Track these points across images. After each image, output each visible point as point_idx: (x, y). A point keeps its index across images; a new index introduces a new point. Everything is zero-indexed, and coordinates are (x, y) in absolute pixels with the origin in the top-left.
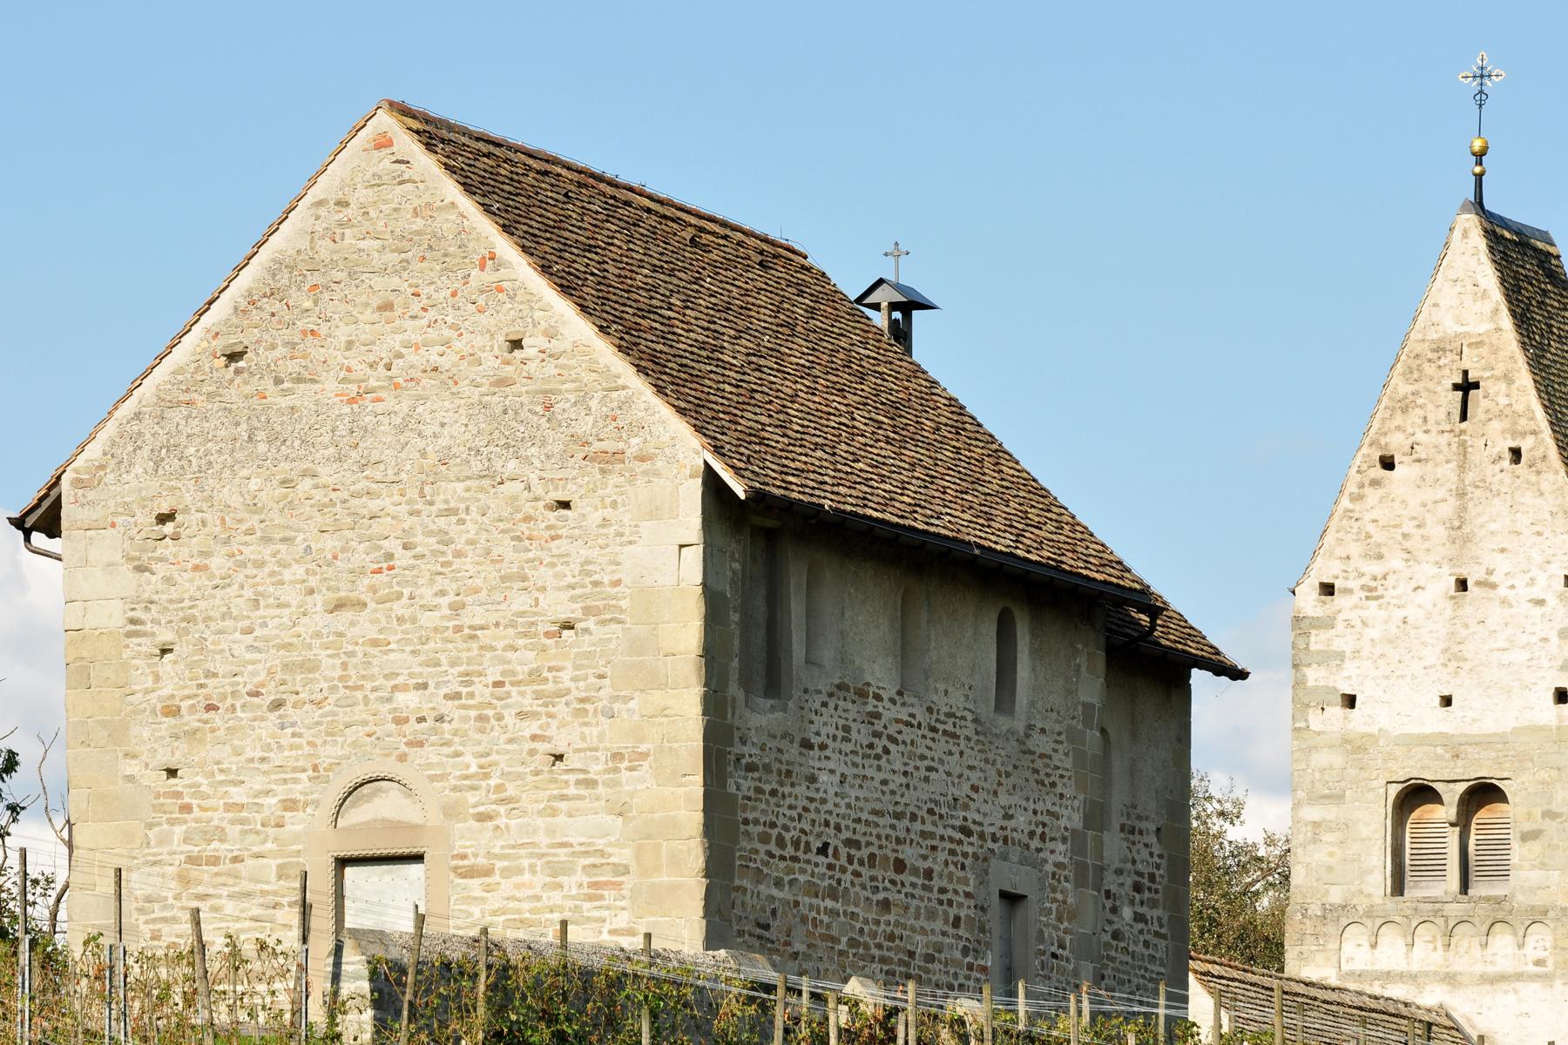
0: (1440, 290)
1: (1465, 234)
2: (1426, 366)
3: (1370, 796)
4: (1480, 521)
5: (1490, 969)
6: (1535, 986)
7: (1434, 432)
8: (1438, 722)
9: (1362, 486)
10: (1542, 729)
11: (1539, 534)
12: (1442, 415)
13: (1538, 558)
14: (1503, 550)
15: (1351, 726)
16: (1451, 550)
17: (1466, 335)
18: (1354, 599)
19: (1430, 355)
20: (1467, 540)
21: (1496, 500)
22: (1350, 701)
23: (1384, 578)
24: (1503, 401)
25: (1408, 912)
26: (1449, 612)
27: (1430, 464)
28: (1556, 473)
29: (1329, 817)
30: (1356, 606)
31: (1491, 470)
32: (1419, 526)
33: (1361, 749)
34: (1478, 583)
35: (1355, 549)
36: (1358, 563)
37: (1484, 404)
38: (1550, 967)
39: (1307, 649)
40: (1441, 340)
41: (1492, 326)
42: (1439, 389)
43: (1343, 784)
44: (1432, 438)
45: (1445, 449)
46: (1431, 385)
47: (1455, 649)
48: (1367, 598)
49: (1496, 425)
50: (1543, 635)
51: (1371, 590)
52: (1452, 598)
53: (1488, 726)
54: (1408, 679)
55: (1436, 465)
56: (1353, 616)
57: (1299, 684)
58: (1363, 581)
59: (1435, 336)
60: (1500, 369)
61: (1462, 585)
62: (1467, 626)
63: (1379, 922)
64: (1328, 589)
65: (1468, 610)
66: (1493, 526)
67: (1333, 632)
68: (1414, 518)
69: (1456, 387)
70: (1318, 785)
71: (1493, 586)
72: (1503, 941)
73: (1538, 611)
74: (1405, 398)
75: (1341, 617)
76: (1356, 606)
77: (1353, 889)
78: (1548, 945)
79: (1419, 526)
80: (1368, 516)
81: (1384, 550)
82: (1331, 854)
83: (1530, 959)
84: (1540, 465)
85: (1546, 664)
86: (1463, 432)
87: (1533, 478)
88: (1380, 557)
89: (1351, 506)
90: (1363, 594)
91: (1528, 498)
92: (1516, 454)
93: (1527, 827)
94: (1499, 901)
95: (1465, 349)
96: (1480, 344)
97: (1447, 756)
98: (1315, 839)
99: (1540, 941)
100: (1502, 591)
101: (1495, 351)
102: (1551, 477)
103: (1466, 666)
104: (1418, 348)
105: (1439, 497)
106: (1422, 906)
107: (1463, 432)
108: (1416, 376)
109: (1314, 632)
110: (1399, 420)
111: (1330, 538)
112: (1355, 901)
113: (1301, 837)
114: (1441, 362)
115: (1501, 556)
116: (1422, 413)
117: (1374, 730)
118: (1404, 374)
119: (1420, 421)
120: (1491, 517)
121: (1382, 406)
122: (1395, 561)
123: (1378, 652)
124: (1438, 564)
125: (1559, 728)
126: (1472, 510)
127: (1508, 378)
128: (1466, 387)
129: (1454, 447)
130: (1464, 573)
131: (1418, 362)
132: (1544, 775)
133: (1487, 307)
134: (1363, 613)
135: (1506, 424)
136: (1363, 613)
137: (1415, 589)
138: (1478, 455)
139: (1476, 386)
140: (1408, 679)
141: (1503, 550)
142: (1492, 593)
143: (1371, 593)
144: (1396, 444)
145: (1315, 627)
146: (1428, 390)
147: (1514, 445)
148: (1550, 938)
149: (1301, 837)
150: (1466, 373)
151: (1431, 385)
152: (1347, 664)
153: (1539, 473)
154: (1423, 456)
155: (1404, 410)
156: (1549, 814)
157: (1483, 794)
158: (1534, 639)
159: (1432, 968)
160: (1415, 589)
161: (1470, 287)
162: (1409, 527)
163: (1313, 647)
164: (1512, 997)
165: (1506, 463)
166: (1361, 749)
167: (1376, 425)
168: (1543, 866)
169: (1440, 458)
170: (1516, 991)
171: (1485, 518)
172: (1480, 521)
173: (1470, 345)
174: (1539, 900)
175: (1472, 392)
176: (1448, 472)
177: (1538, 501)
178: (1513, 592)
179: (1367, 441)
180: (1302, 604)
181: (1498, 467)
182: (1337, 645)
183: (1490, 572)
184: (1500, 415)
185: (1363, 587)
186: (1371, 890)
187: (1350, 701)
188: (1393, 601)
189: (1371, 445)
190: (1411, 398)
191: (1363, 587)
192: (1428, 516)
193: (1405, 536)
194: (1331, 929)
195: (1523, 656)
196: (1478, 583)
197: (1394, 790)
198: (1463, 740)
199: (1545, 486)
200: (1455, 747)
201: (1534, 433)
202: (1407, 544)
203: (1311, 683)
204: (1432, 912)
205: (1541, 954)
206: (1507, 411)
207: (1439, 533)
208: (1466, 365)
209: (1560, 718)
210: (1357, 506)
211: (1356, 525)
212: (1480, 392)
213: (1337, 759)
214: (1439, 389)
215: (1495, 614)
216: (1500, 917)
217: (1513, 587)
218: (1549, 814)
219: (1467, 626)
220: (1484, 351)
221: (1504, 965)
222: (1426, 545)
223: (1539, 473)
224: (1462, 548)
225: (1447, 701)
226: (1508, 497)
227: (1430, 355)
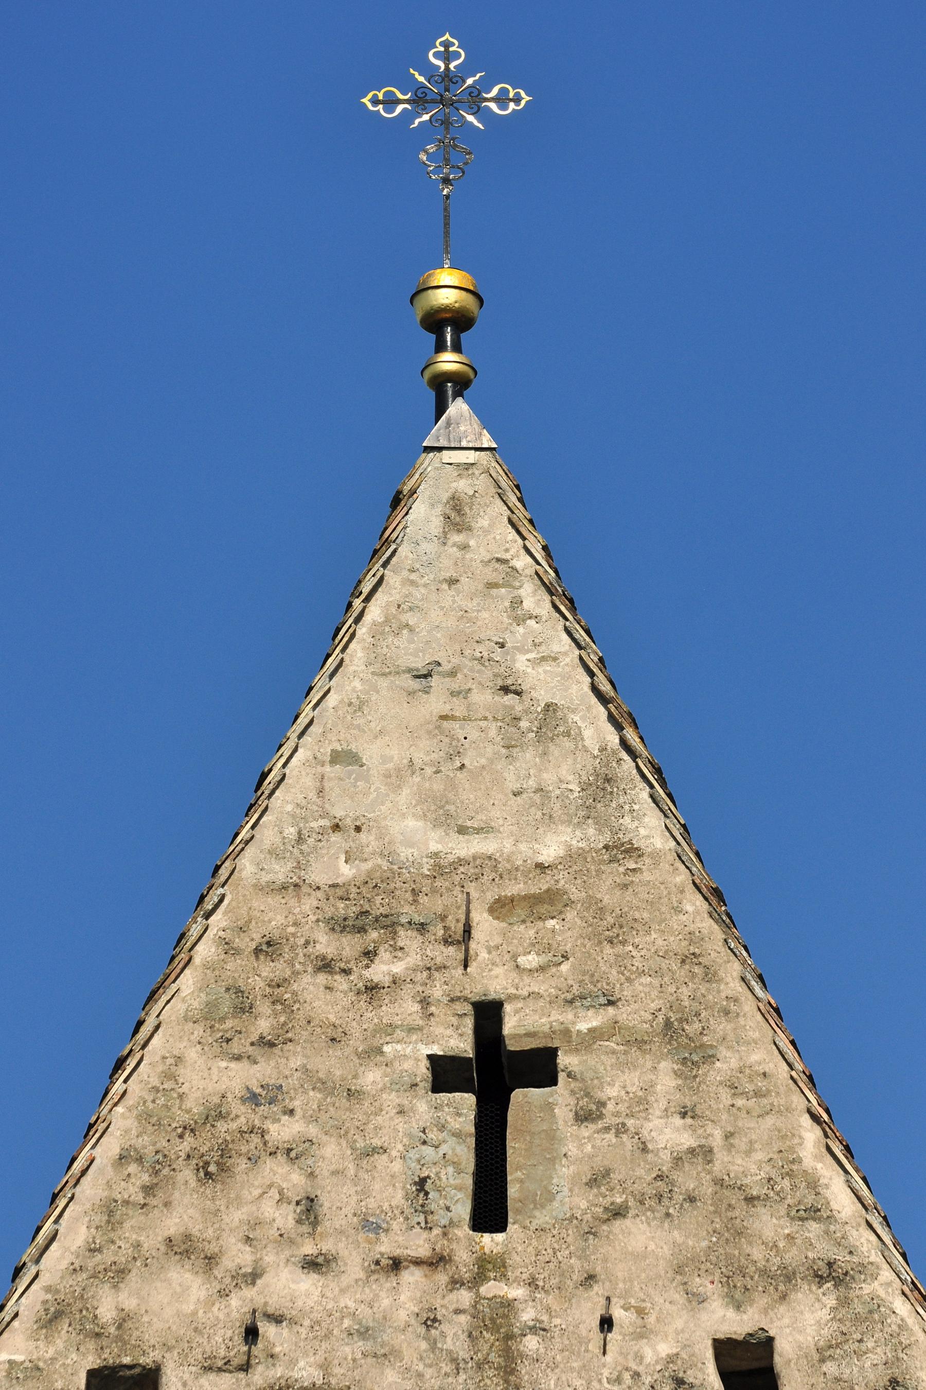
1: (457, 516)
2: (310, 986)
7: (353, 1265)
12: (388, 1192)
17: (484, 865)
19: (326, 944)
24: (669, 1135)
37: (581, 1146)
40: (374, 883)
41: (593, 837)
42: (371, 1078)
44: (345, 1294)
45: (412, 1346)
46: (331, 1064)
49: (640, 1235)
59: (346, 871)
60: (641, 1007)
69: (445, 1074)
74: (216, 1114)
86: (488, 1267)
96: (544, 904)
101: (614, 931)
104: (274, 917)
108: (264, 1026)
110: (184, 1212)
114: (382, 969)
116: (294, 1180)
118: (208, 1015)
119: (285, 1218)
127: (682, 1041)
128: (495, 1071)
129: (454, 1335)
131: (269, 969)
133: (564, 772)
135: (692, 1235)
139: (540, 1067)
146: (324, 1085)
147: (737, 1324)
150: (488, 1015)
151: (331, 1064)
155: (213, 1170)
161: (484, 698)
173: (501, 907)
175: (524, 1100)
184: (662, 1196)
189: (50, 1319)
190: (243, 1116)
201: (829, 1274)
206: (689, 1179)
208: (493, 981)
212: (560, 1097)
214: (371, 1078)
220: (563, 929)
227: (326, 944)
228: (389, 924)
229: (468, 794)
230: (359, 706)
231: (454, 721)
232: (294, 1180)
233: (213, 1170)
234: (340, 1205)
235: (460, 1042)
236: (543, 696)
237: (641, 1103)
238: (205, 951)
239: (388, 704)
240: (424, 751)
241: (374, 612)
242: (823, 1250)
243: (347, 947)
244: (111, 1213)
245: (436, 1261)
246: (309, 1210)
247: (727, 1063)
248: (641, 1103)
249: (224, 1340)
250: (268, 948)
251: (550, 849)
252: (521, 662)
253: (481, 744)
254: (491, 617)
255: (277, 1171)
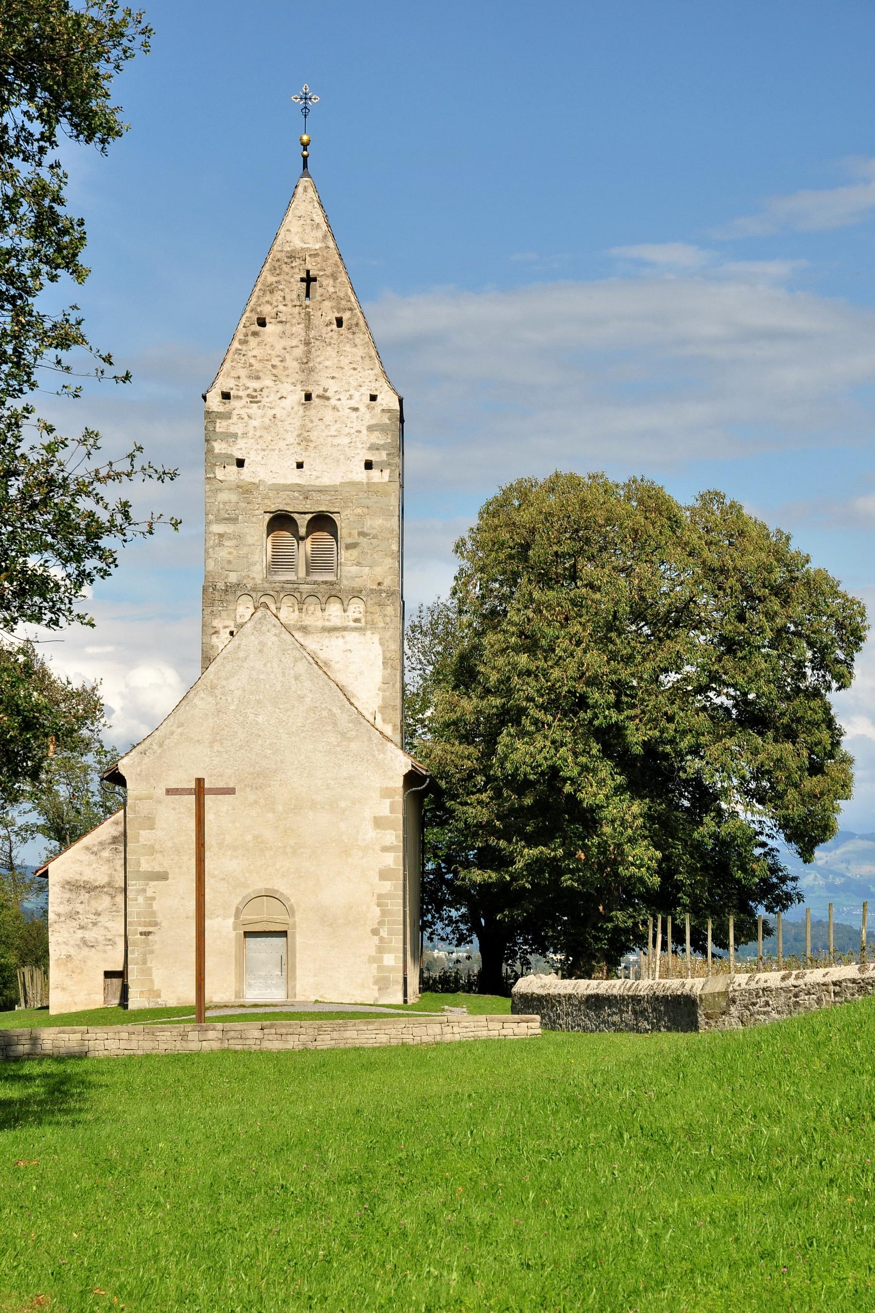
0: (291, 222)
1: (305, 190)
2: (284, 266)
3: (254, 519)
4: (319, 360)
5: (327, 624)
6: (355, 634)
7: (290, 306)
8: (294, 477)
9: (246, 335)
10: (359, 483)
11: (354, 369)
13: (354, 384)
14: (333, 378)
15: (242, 478)
16: (302, 377)
17: (308, 249)
18: (243, 402)
19: (286, 260)
20: (311, 370)
21: (329, 348)
22: (240, 463)
23: (261, 390)
24: (331, 290)
25: (278, 589)
26: (301, 412)
27: (288, 325)
28: (364, 334)
29: (228, 531)
30: (244, 407)
31: (324, 330)
32: (282, 361)
33: (248, 492)
34: (318, 396)
35: (243, 373)
36: (244, 381)
37: (320, 290)
38: (362, 624)
39: (214, 431)
40: (293, 251)
42: (292, 280)
43: (237, 512)
45: (297, 316)
46: (287, 278)
47: (306, 434)
48: (251, 402)
49: (327, 304)
50: (358, 429)
51: (253, 397)
52: (303, 404)
53: (326, 480)
54: (277, 452)
55: (292, 325)
56: (243, 412)
57: (210, 451)
58: (248, 392)
59: (289, 249)
61: (308, 397)
62: (312, 421)
63: (260, 594)
64: (226, 396)
65: (312, 412)
66: (327, 363)
67: (230, 421)
68: (279, 356)
69: (302, 280)
70: (222, 512)
71: (328, 399)
72: (334, 608)
73: (354, 415)
74: (272, 284)
75: (235, 412)
76: (244, 407)
77: (243, 574)
78: (362, 610)
79: (282, 361)
80: (250, 354)
81: (261, 374)
82: (230, 553)
83: (351, 618)
84: (354, 329)
85: (359, 445)
86: (307, 307)
87: (351, 336)
88: (258, 378)
89: (240, 347)
90: (249, 400)
91: (348, 348)
92: (340, 322)
93: (349, 541)
94: (332, 584)
95: (308, 258)
96: (316, 255)
97: (301, 498)
98: (220, 545)
99: (356, 608)
100: (333, 402)
101: (326, 260)
102: (361, 336)
103: (312, 445)
104: (279, 255)
105: (294, 344)
106: (285, 585)
107: (307, 307)
109: (218, 421)
110: (268, 297)
111: (227, 365)
112: (245, 582)
113: (211, 542)
114: (294, 264)
115: (331, 381)
116: (282, 294)
117: (256, 481)
118: (270, 270)
119: (281, 299)
120: (326, 358)
121: (257, 288)
122: (267, 382)
123: (258, 434)
124: (294, 384)
125: (368, 484)
126: (314, 353)
127: (334, 277)
129: (303, 315)
130: (310, 389)
131: (278, 263)
132: (359, 511)
133: (320, 234)
134: (248, 410)
135: (333, 303)
136: (249, 411)
137: (280, 398)
138: (317, 321)
139: (315, 280)
140: (277, 452)
141: (333, 378)
142: (327, 403)
143: (253, 399)
144: (267, 310)
145: (219, 418)
147: (338, 315)
148: (363, 606)
149: (211, 542)
150: (308, 272)
151: (287, 278)
152: (239, 440)
153: (354, 333)
154: (284, 319)
155: (272, 292)
156: (362, 534)
157: (323, 522)
158: (353, 431)
159: (292, 622)
160: (280, 398)
161: (309, 221)
162: (276, 361)
163: (218, 430)
164: (341, 640)
165: (334, 327)
166: (248, 492)
167: (254, 299)
168: (358, 564)
169: (294, 321)
170: (343, 637)
171: (322, 358)
172: (319, 360)
173: (310, 255)
174: (357, 584)
176: (299, 329)
177: (354, 350)
178: (339, 402)
179: (249, 308)
180: (211, 404)
181: (329, 328)
182: (233, 429)
183: (325, 390)
184: (330, 298)
185: (248, 396)
186: (255, 575)
187: (240, 463)
188: (267, 405)
189: (252, 311)
190: (275, 285)
191: (248, 396)
192: (287, 356)
193: (273, 366)
194: (230, 597)
195: (345, 441)
196: (318, 396)
197: (268, 517)
198: (311, 488)
199: (357, 341)
200: (306, 492)
201: (351, 309)
202: (274, 371)
203: (217, 451)
204: (292, 591)
205: (358, 616)
207: (293, 365)
208: (309, 267)
209: (368, 477)
210: (244, 347)
211: (243, 358)
213: (234, 497)
214: (292, 280)
215: (329, 415)
216: (334, 593)
217: (339, 399)
218: (362, 534)
219: (312, 421)
220: (319, 259)
221: (336, 622)
222: (287, 373)
223: (354, 333)
224: (309, 374)
225: (300, 465)
226: (336, 346)
227: (286, 260)
228: (295, 257)
229: (306, 237)
230: (291, 222)
231: (303, 227)
232: (282, 294)
233: (272, 292)
234: (288, 297)
235: (305, 276)
236: (317, 221)
237: (328, 285)
238: (270, 260)
239: (295, 221)
240: (300, 230)
241: (293, 206)
242: (349, 305)
243: (289, 260)
244: (258, 297)
245: (301, 306)
246: (284, 298)
247: (340, 280)
248: (328, 285)
249: (274, 314)
250: (278, 260)
251: (317, 247)
252: (314, 216)
253: (308, 229)
254: (310, 207)
255: (280, 292)
